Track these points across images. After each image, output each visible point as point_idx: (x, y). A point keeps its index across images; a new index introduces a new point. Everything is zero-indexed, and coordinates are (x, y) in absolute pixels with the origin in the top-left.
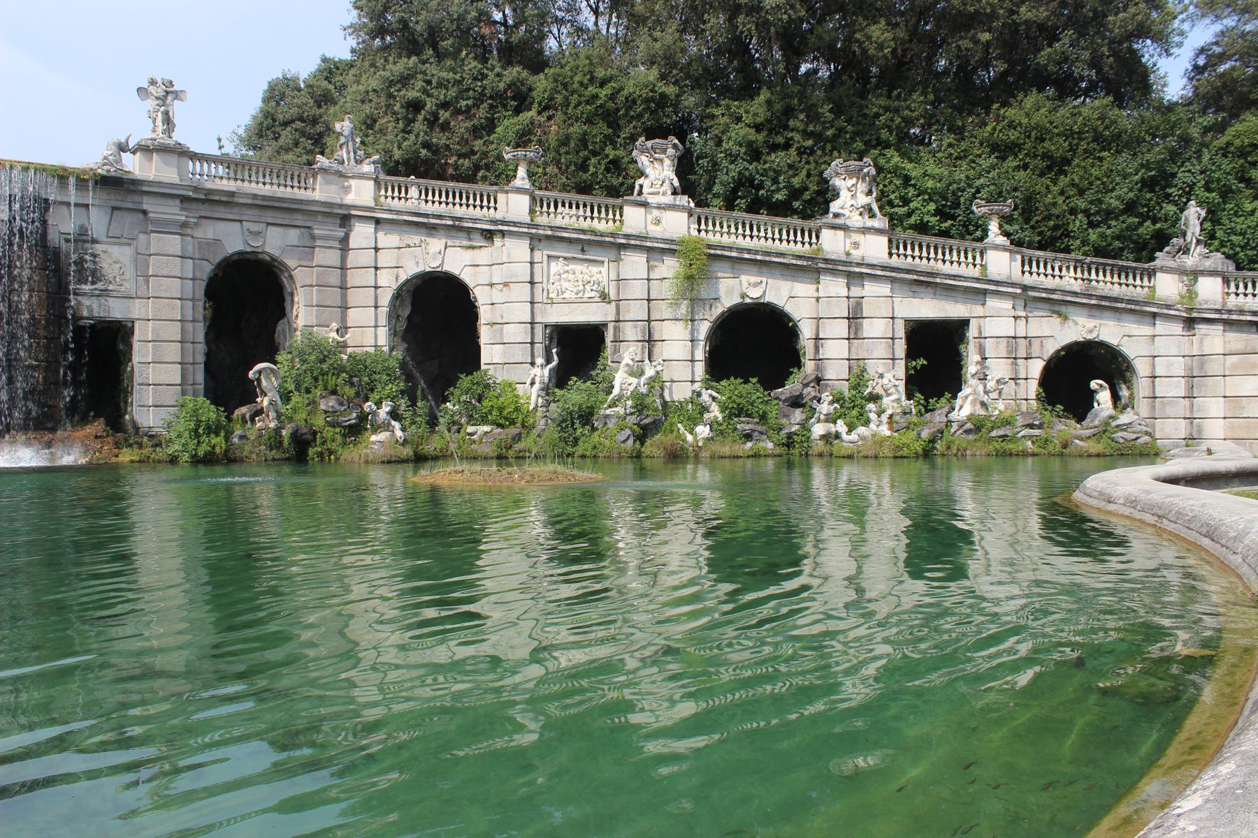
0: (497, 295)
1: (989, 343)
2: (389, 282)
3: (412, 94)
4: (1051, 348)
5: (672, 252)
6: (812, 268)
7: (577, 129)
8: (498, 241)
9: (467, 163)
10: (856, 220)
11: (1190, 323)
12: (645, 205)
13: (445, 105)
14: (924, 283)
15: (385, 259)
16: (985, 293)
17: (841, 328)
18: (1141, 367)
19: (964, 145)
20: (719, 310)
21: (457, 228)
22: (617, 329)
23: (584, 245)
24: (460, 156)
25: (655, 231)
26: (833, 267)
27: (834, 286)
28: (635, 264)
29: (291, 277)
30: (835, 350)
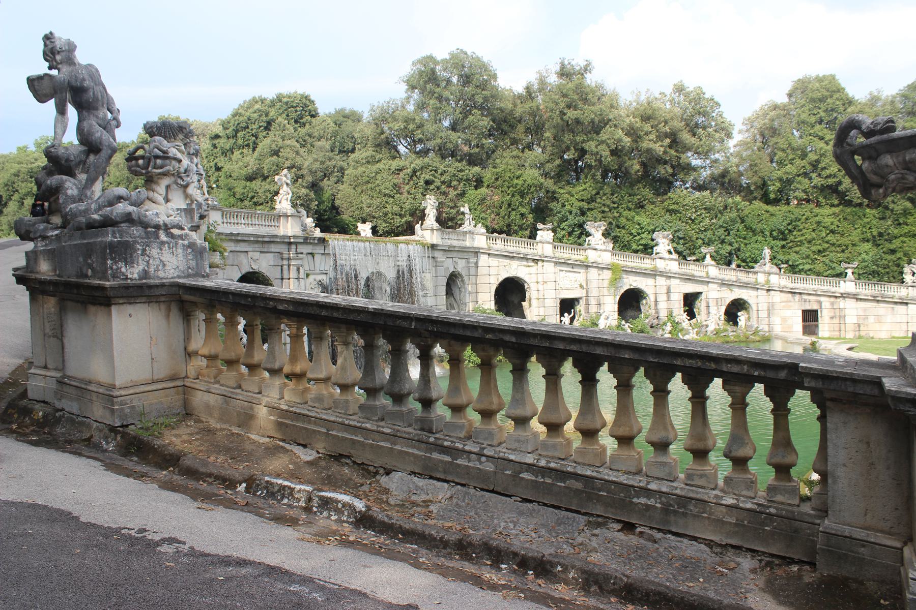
0: (540, 287)
1: (710, 301)
2: (495, 282)
3: (428, 177)
4: (728, 301)
5: (608, 269)
6: (654, 274)
7: (508, 198)
8: (540, 263)
9: (454, 211)
10: (667, 255)
11: (768, 290)
12: (595, 249)
13: (443, 183)
14: (690, 279)
15: (493, 271)
16: (709, 282)
17: (664, 297)
18: (754, 307)
19: (657, 209)
20: (622, 291)
21: (525, 258)
22: (587, 300)
23: (573, 266)
24: (452, 208)
25: (599, 260)
26: (662, 274)
27: (661, 281)
28: (593, 272)
29: (463, 281)
30: (663, 305)
